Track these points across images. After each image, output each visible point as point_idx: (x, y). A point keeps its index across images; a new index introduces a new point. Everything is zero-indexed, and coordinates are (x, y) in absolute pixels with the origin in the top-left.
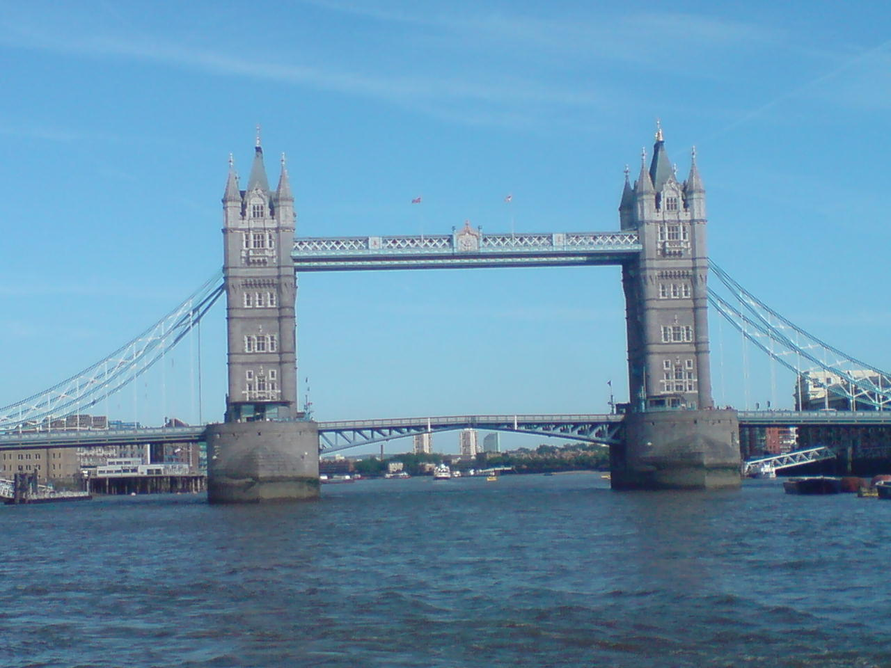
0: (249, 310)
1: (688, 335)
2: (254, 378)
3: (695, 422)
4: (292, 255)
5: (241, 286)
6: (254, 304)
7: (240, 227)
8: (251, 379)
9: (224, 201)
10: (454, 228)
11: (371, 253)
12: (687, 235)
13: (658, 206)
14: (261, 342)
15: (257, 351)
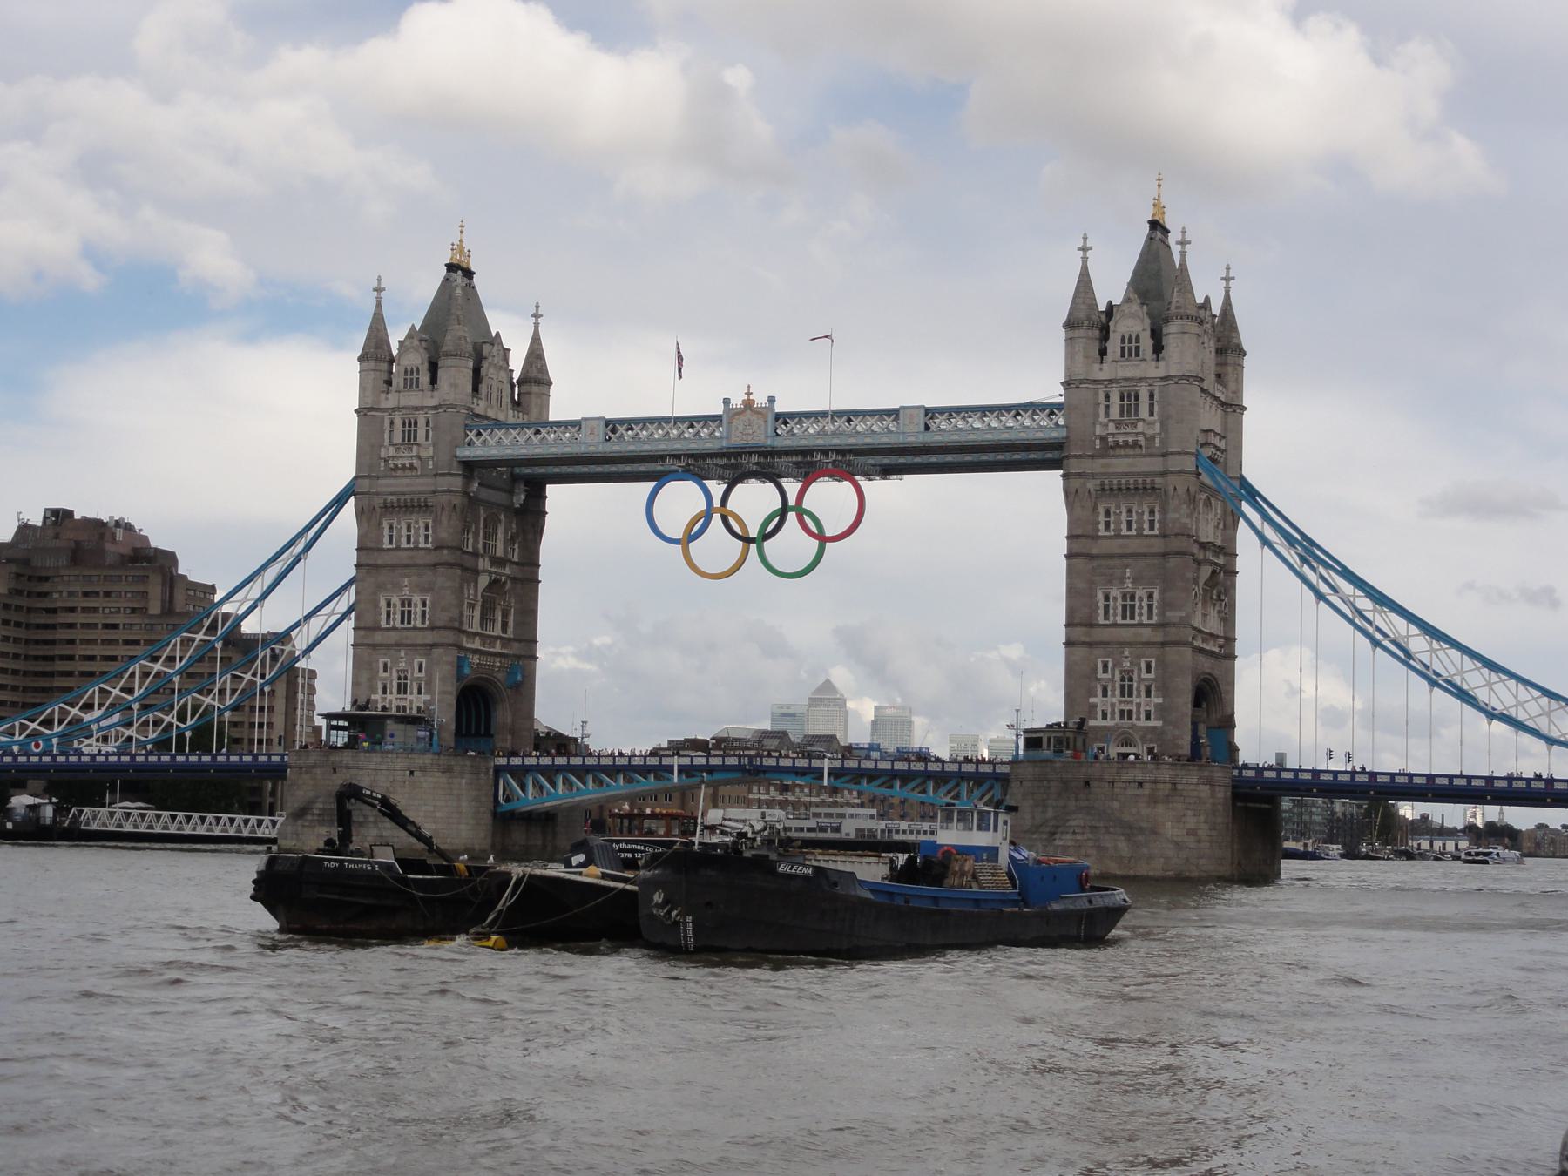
0: (391, 553)
1: (1150, 607)
2: (391, 673)
3: (1087, 783)
4: (458, 454)
5: (378, 510)
6: (399, 541)
7: (383, 405)
8: (388, 675)
9: (360, 359)
10: (726, 402)
11: (583, 449)
12: (1156, 408)
13: (1103, 352)
14: (406, 609)
15: (398, 625)
